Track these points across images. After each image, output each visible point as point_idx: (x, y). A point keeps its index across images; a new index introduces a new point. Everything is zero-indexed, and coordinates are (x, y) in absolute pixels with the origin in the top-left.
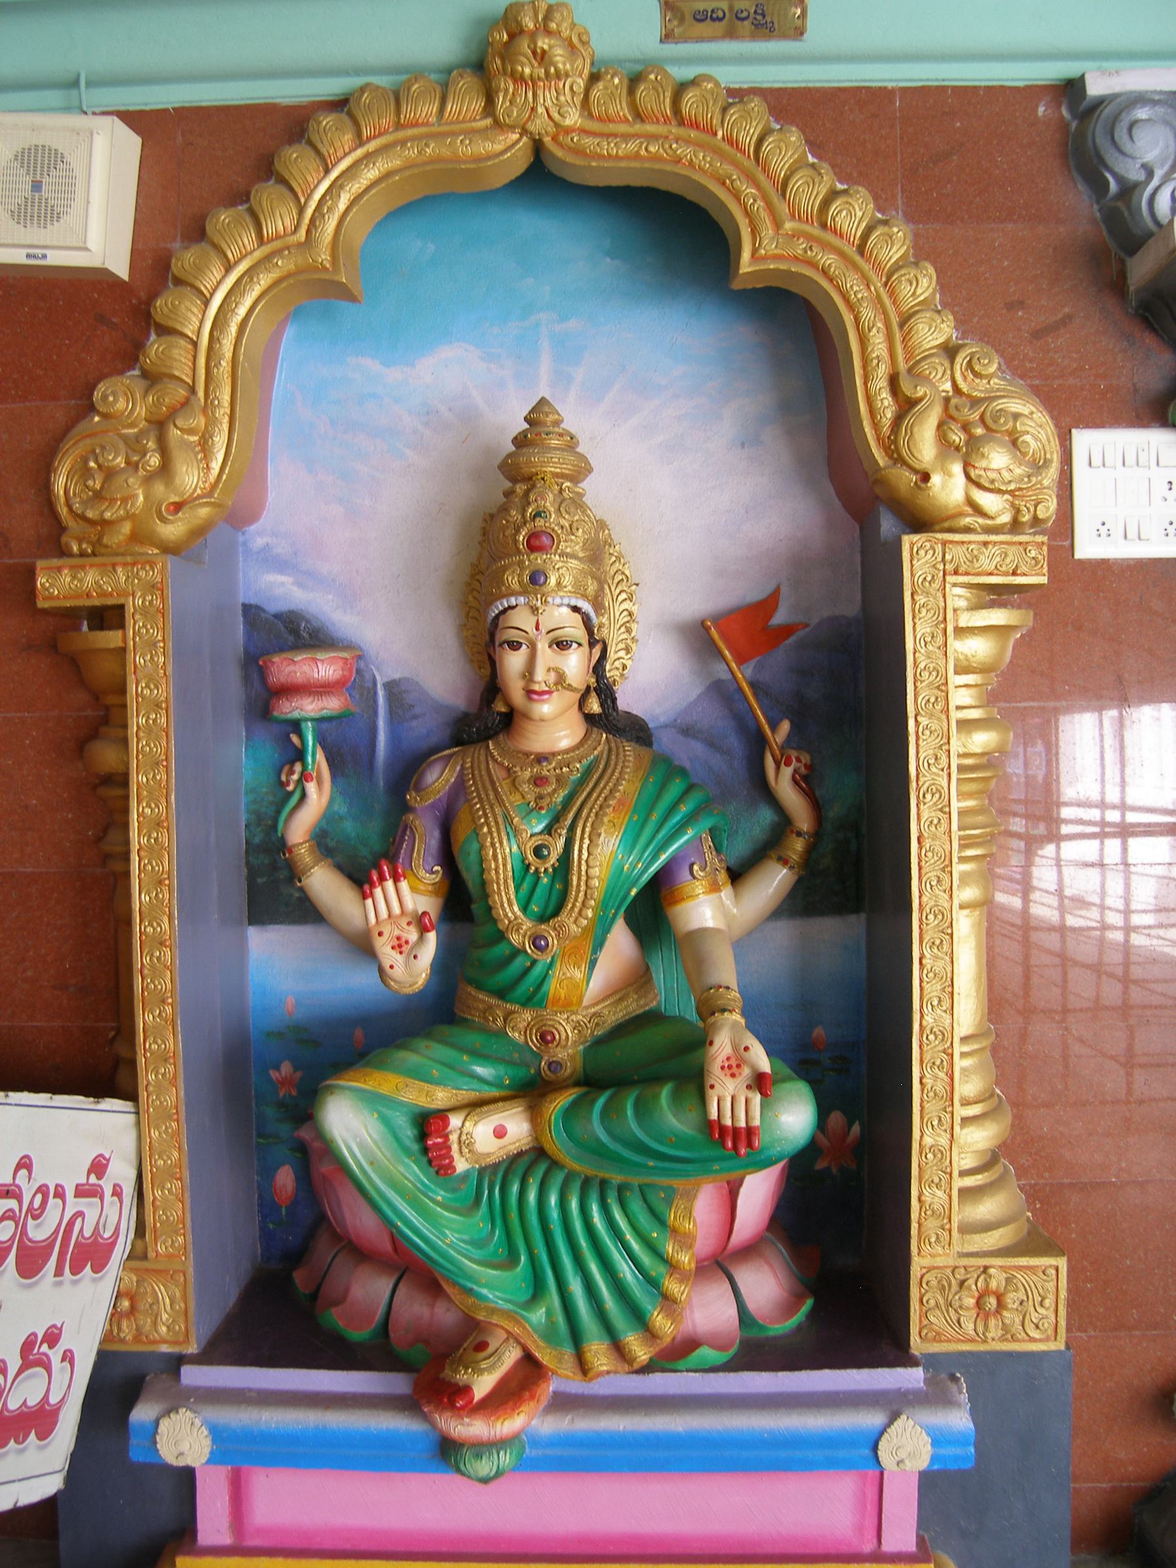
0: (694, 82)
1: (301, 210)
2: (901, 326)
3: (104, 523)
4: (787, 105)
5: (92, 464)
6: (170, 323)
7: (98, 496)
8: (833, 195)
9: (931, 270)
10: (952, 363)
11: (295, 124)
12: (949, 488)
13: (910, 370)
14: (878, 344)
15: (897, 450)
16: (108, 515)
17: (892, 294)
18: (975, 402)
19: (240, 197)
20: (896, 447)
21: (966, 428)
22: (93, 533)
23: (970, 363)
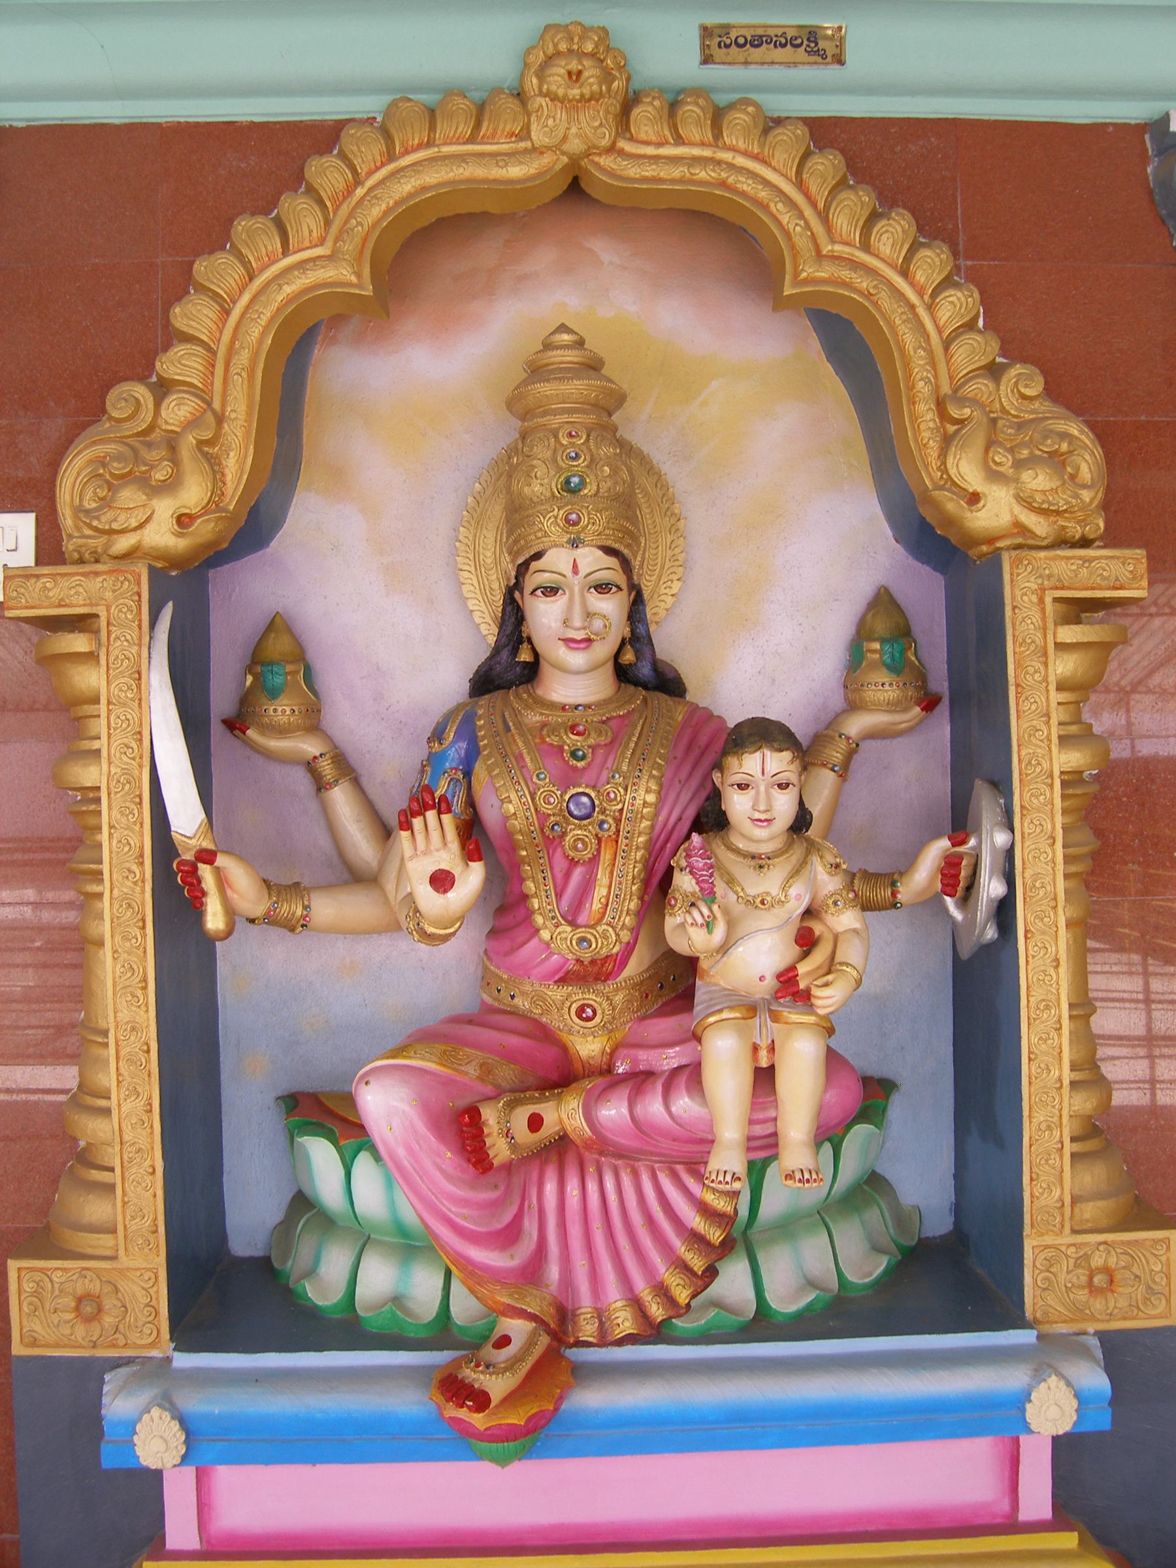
1: (328, 223)
2: (946, 349)
3: (111, 532)
7: (106, 503)
8: (873, 217)
12: (996, 510)
13: (955, 391)
16: (115, 526)
18: (1021, 426)
19: (266, 206)
21: (1011, 450)
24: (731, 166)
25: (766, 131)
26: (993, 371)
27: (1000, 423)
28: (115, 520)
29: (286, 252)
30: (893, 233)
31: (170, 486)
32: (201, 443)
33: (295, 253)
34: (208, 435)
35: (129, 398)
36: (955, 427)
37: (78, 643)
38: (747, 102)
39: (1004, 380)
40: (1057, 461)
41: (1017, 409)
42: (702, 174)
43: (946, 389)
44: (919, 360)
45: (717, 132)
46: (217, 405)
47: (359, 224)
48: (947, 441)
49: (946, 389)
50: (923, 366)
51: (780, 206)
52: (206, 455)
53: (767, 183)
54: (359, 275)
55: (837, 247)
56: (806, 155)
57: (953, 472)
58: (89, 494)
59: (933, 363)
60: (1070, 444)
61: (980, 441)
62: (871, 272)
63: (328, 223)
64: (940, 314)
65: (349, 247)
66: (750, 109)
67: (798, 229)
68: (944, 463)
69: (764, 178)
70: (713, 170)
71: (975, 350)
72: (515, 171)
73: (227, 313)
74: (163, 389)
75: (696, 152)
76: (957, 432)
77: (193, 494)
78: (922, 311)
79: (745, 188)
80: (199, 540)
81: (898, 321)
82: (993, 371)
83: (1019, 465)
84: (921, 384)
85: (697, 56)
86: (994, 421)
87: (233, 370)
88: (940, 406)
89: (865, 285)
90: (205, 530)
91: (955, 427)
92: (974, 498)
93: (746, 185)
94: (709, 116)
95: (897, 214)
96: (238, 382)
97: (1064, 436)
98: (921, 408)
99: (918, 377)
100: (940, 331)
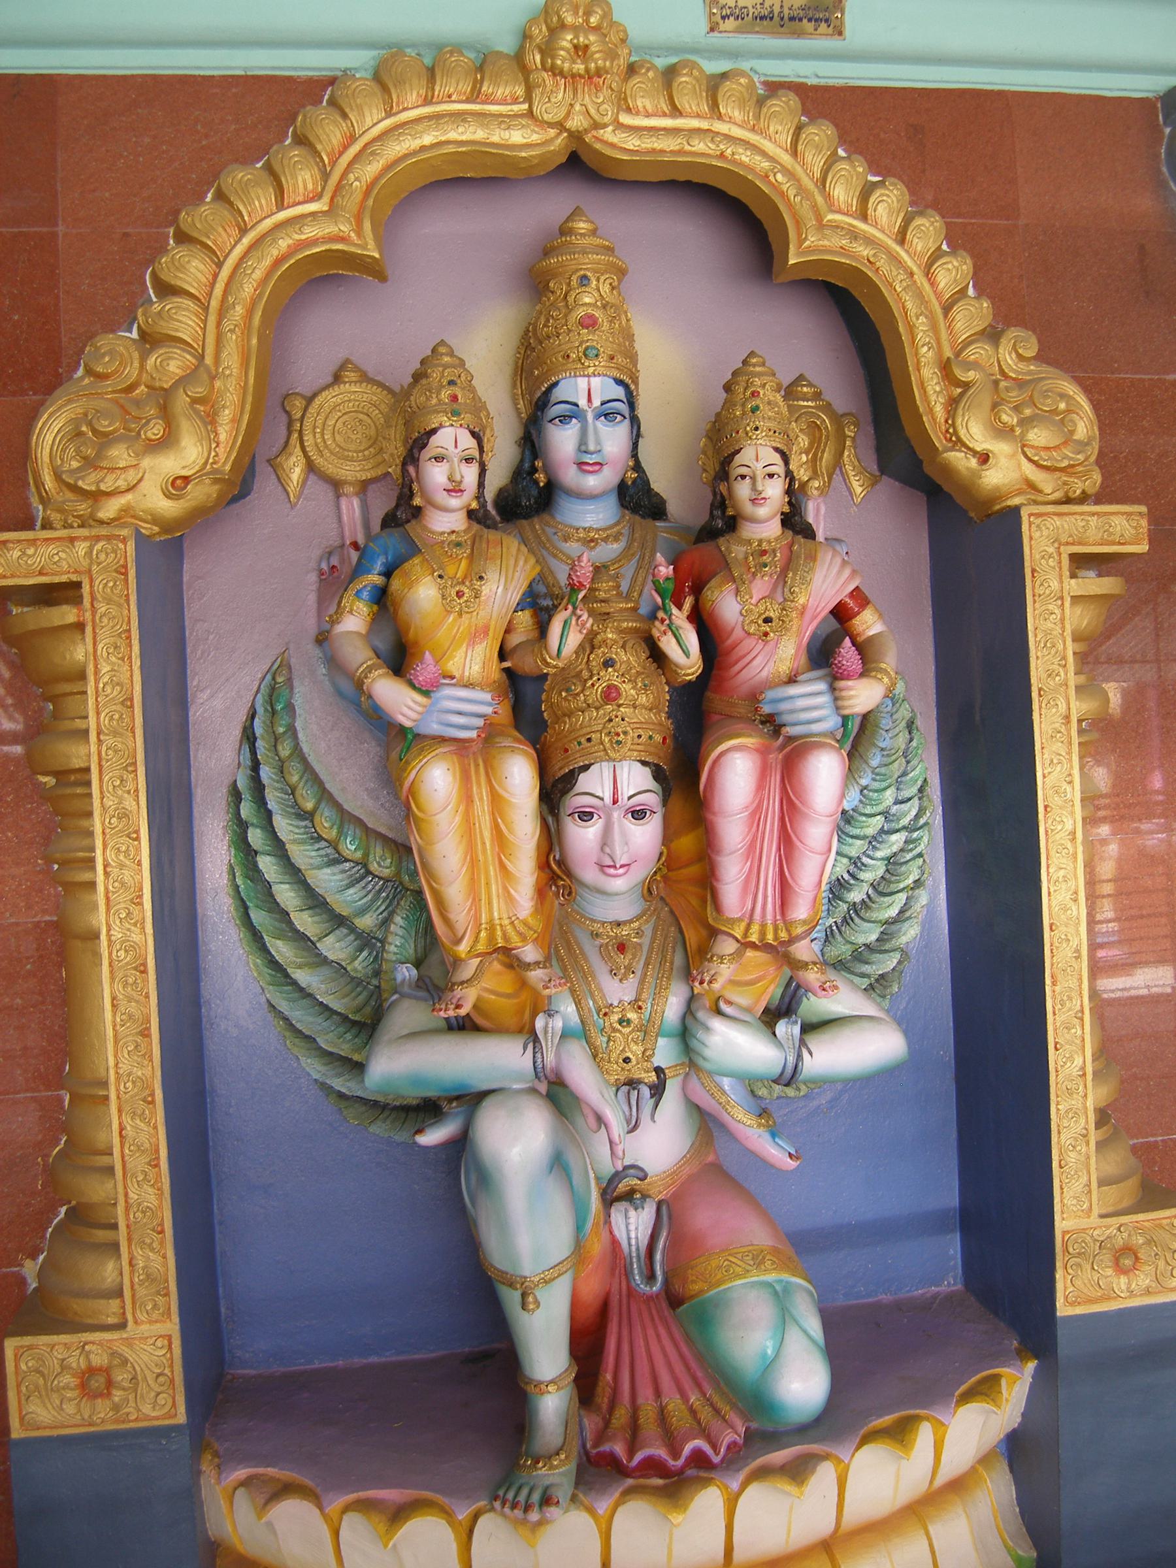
0: (724, 76)
3: (98, 496)
4: (817, 101)
5: (84, 429)
6: (179, 283)
7: (90, 464)
9: (969, 261)
10: (997, 347)
11: (317, 90)
13: (958, 355)
14: (922, 333)
15: (956, 433)
16: (103, 487)
17: (933, 284)
20: (955, 430)
21: (1017, 409)
22: (83, 507)
23: (1014, 348)
24: (728, 138)
25: (760, 102)
26: (992, 335)
27: (1003, 384)
28: (102, 480)
29: (281, 206)
30: (889, 203)
31: (167, 442)
32: (195, 401)
33: (289, 207)
34: (199, 391)
35: (116, 350)
36: (959, 390)
37: (67, 614)
38: (742, 73)
39: (1003, 341)
40: (1062, 421)
41: (1015, 371)
42: (699, 146)
43: (948, 353)
44: (922, 324)
45: (714, 105)
46: (209, 360)
47: (357, 179)
48: (953, 404)
49: (948, 353)
50: (924, 332)
51: (779, 177)
52: (196, 412)
53: (763, 153)
54: (359, 231)
55: (838, 217)
56: (799, 129)
57: (962, 433)
58: (71, 451)
59: (934, 328)
60: (1067, 404)
61: (986, 400)
62: (869, 241)
63: (326, 176)
64: (939, 278)
65: (352, 201)
66: (742, 81)
67: (798, 199)
68: (953, 425)
69: (763, 149)
70: (712, 141)
71: (973, 315)
72: (517, 137)
73: (220, 265)
74: (150, 340)
75: (695, 123)
76: (962, 395)
77: (189, 454)
78: (919, 278)
79: (744, 158)
80: (194, 503)
81: (899, 290)
82: (992, 335)
83: (1025, 423)
84: (925, 349)
85: (704, 26)
86: (996, 383)
87: (227, 325)
88: (945, 368)
89: (865, 253)
90: (201, 493)
91: (959, 390)
92: (984, 458)
93: (745, 157)
94: (704, 87)
95: (891, 184)
96: (232, 340)
97: (1063, 396)
98: (927, 372)
99: (921, 343)
100: (938, 296)
